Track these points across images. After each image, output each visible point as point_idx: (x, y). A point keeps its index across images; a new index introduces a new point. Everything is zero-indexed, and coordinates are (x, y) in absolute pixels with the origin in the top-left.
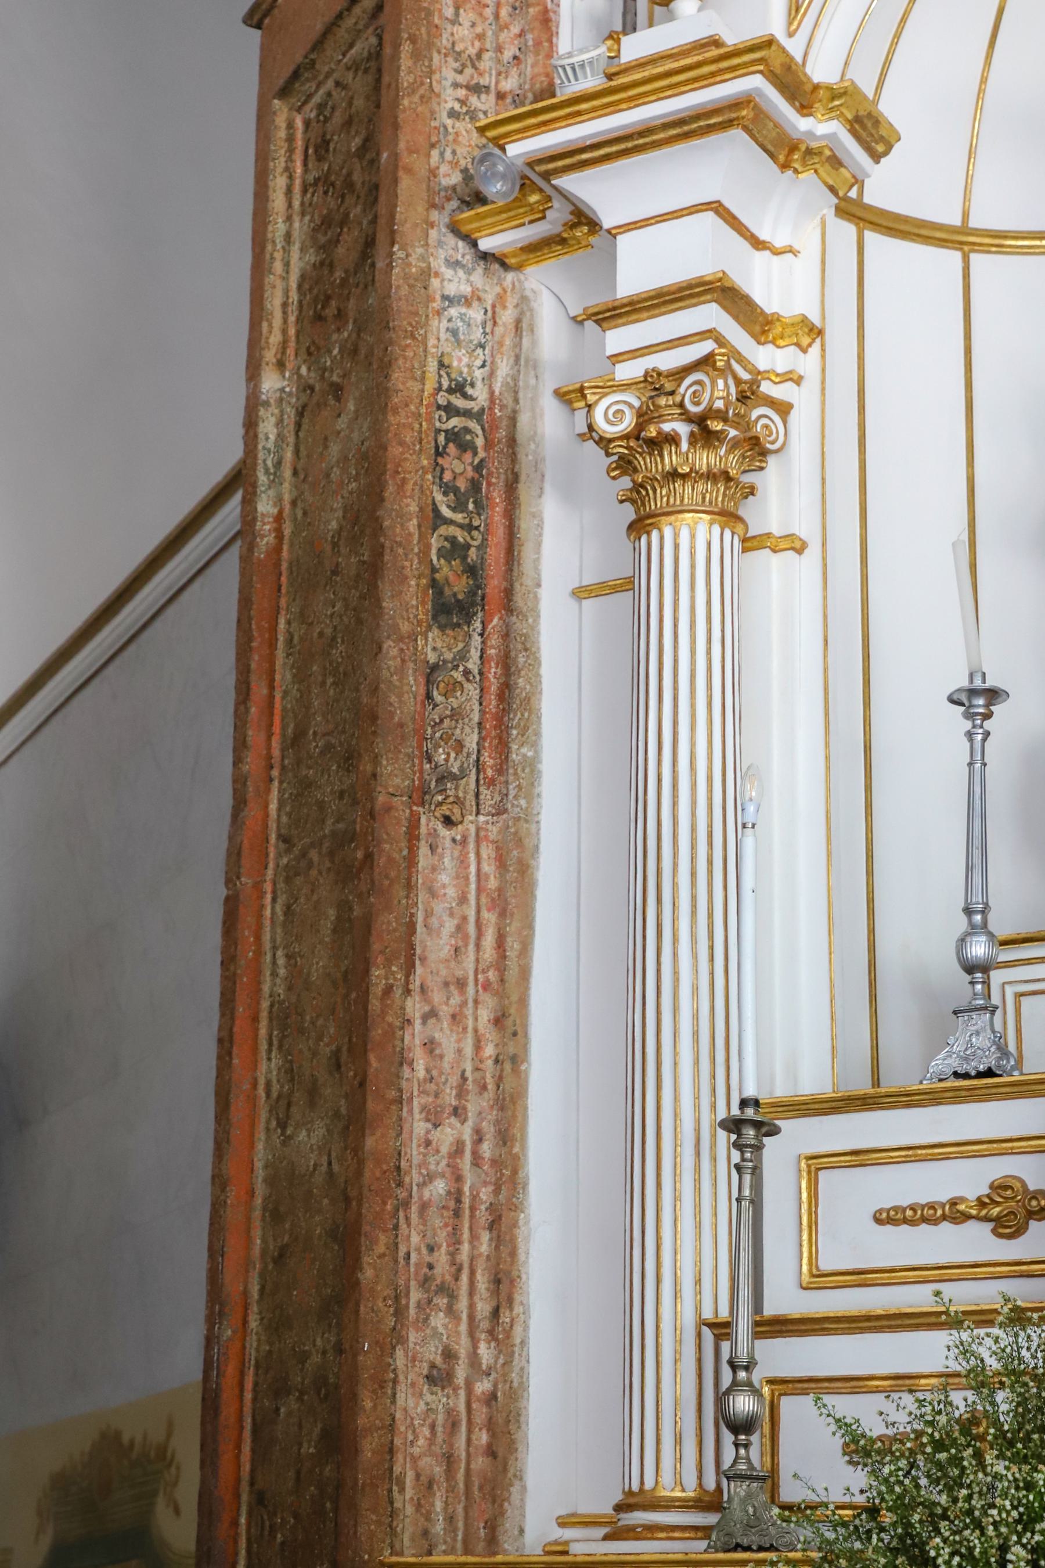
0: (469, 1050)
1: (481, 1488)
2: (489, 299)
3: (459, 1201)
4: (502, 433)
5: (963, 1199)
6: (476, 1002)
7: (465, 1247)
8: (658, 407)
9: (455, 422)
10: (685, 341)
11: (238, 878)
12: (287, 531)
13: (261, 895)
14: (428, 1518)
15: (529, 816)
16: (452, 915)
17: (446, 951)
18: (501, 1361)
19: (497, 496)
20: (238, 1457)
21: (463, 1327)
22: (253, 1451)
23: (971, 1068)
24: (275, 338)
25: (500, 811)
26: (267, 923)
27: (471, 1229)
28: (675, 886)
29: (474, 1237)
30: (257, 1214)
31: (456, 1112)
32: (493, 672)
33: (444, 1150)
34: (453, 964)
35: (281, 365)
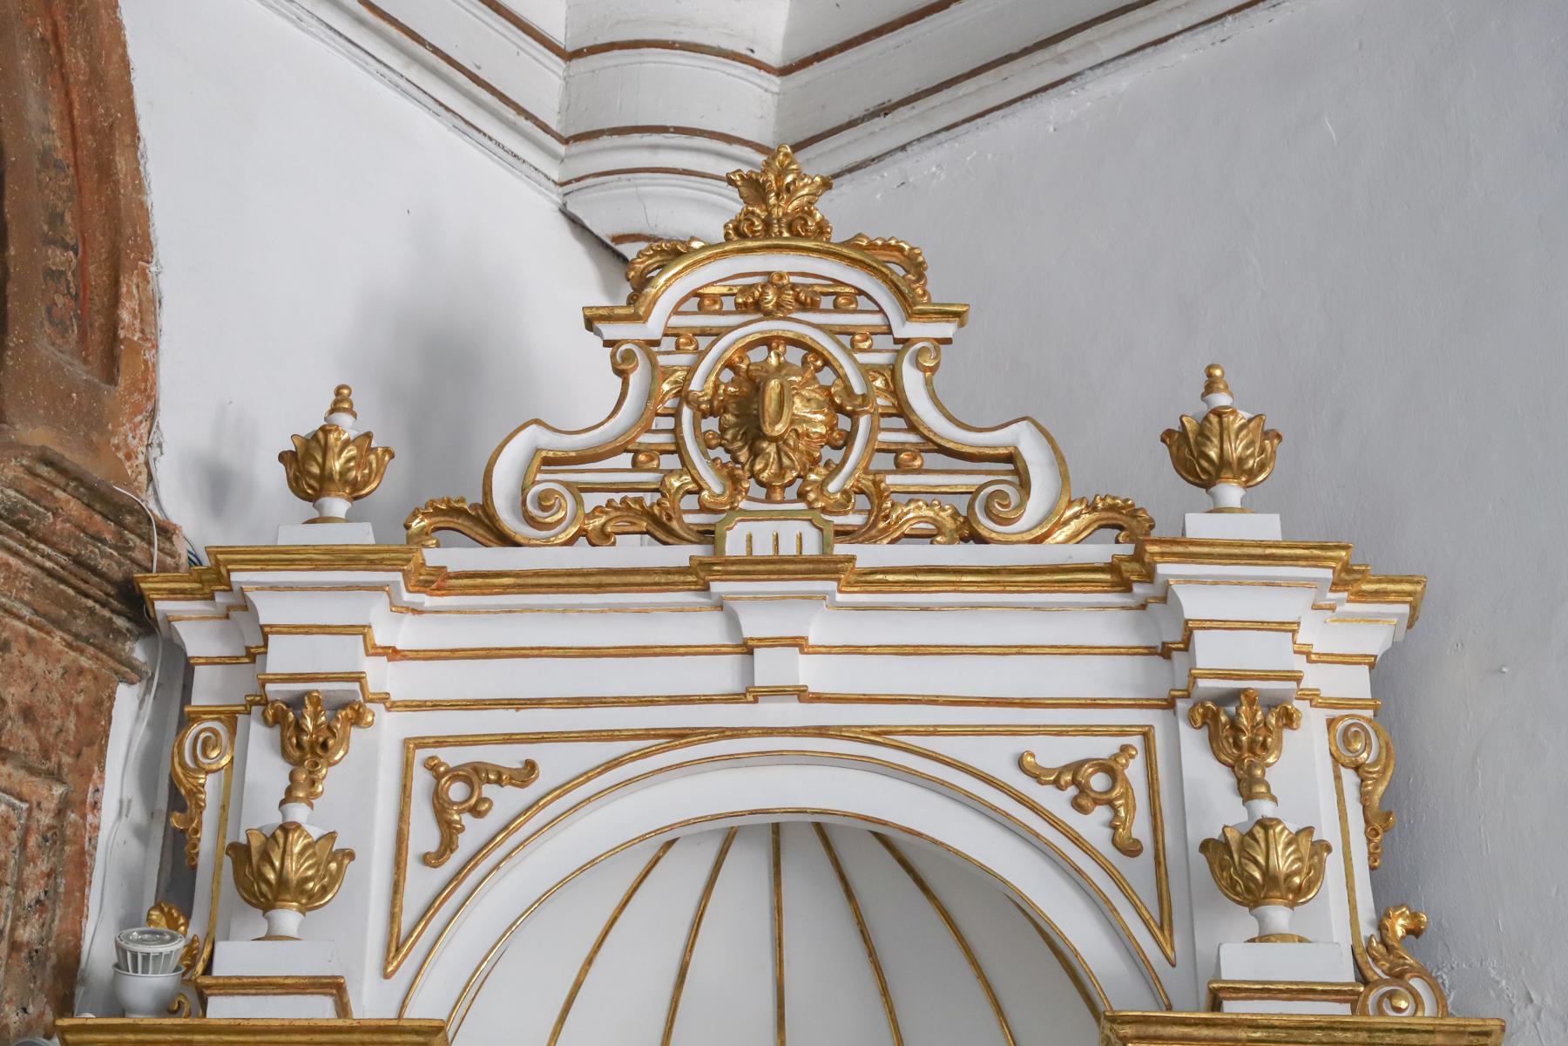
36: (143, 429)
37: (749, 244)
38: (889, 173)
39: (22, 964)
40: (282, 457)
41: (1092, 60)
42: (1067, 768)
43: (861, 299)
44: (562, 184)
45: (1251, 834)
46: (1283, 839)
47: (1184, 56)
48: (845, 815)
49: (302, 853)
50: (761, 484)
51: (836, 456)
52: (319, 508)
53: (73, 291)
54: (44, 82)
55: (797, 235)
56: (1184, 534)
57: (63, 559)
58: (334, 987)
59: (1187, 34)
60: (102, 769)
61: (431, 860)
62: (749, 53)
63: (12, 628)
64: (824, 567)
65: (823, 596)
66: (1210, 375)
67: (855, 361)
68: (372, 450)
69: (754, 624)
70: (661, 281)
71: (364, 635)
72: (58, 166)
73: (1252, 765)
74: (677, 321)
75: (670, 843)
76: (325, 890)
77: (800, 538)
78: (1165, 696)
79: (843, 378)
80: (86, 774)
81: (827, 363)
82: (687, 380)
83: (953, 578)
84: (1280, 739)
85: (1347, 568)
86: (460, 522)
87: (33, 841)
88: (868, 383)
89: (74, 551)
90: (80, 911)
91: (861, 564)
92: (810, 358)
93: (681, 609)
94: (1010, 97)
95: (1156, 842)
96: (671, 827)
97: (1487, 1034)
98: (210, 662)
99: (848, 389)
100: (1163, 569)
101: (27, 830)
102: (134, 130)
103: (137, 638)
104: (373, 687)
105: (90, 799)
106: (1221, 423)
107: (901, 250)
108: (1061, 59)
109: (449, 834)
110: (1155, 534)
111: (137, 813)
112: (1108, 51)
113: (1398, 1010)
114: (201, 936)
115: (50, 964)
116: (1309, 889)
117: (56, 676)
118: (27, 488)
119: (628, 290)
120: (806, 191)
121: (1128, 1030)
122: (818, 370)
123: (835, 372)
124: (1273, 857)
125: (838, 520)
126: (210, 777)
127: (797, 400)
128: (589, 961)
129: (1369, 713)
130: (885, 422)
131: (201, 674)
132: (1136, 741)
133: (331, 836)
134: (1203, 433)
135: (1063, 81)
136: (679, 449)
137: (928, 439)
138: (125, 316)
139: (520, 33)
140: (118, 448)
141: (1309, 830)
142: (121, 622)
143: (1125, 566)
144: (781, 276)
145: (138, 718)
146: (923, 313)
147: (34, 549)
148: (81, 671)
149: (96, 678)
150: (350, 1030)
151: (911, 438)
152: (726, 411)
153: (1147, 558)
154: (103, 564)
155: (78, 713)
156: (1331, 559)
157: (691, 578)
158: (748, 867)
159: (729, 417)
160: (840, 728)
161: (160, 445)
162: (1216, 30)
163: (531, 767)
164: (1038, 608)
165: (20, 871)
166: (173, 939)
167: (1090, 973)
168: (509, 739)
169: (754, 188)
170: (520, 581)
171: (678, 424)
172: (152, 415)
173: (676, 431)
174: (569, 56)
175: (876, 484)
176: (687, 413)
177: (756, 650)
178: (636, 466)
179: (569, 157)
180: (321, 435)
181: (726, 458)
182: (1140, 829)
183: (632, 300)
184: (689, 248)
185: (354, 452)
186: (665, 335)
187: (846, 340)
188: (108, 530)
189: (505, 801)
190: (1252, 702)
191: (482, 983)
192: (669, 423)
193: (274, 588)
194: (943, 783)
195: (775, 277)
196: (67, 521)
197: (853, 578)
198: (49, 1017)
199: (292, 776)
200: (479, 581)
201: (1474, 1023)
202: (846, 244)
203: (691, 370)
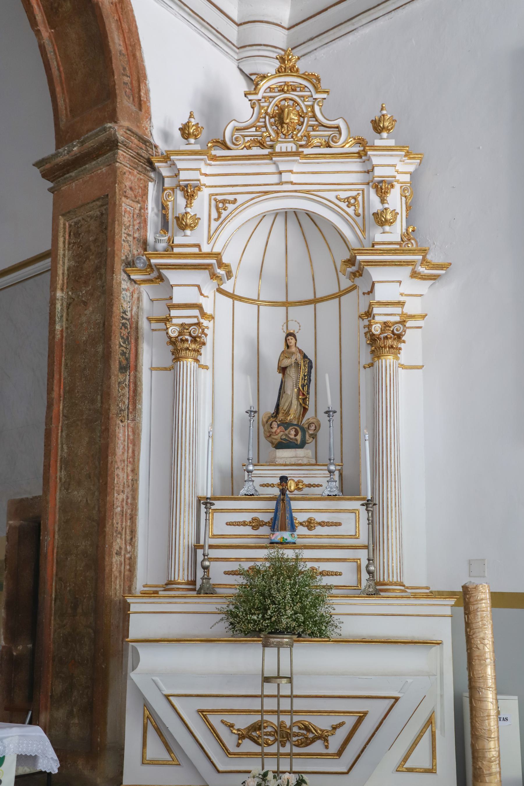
0: (125, 477)
1: (127, 579)
2: (131, 290)
3: (123, 513)
4: (134, 325)
5: (246, 522)
6: (127, 466)
7: (124, 523)
8: (184, 332)
9: (124, 321)
11: (51, 425)
12: (64, 335)
13: (58, 430)
14: (116, 585)
15: (140, 422)
16: (122, 444)
17: (121, 453)
18: (133, 550)
19: (133, 341)
20: (52, 569)
21: (124, 542)
22: (57, 568)
23: (249, 493)
24: (60, 282)
25: (134, 420)
26: (59, 437)
27: (126, 519)
28: (185, 446)
29: (126, 521)
30: (57, 510)
31: (123, 492)
32: (132, 385)
33: (120, 500)
34: (122, 456)
35: (62, 290)
36: (149, 122)
37: (281, 74)
38: (312, 56)
39: (136, 242)
40: (180, 129)
41: (360, 24)
42: (346, 198)
43: (306, 88)
44: (238, 60)
45: (383, 211)
46: (389, 212)
47: (382, 23)
48: (300, 209)
49: (190, 218)
50: (283, 134)
51: (299, 127)
52: (188, 141)
53: (130, 88)
54: (118, 32)
55: (291, 72)
56: (374, 144)
57: (135, 153)
58: (198, 246)
59: (383, 17)
60: (147, 201)
61: (216, 220)
62: (280, 24)
63: (126, 169)
64: (297, 154)
65: (296, 161)
66: (382, 106)
67: (304, 104)
68: (199, 127)
69: (282, 168)
70: (261, 84)
71: (200, 171)
72: (123, 55)
73: (384, 197)
74: (265, 94)
75: (265, 216)
76: (195, 226)
77: (292, 147)
78: (367, 182)
79: (301, 108)
80: (144, 202)
81: (298, 105)
82: (267, 109)
83: (324, 156)
84: (390, 191)
85: (408, 152)
86: (219, 145)
87: (135, 216)
88: (307, 110)
89: (137, 151)
90: (146, 231)
91: (305, 153)
92: (295, 103)
93: (266, 164)
94: (341, 35)
95: (363, 214)
96: (265, 212)
97: (426, 250)
98: (168, 177)
99: (303, 111)
100: (369, 153)
101: (134, 214)
102: (140, 45)
103: (152, 171)
104: (202, 182)
105: (146, 207)
106: (384, 118)
107: (315, 75)
108: (353, 24)
109: (219, 214)
110: (368, 145)
111: (156, 210)
112: (364, 21)
113: (408, 247)
114: (171, 236)
115: (141, 242)
116: (394, 222)
117: (136, 180)
118: (125, 136)
119: (254, 87)
120: (294, 60)
121: (356, 252)
122: (296, 106)
123: (300, 106)
124: (387, 216)
125: (300, 143)
126: (170, 202)
127: (292, 114)
128: (248, 241)
129: (409, 185)
130: (311, 119)
131: (166, 180)
132: (361, 192)
133: (196, 215)
134: (380, 121)
135: (353, 30)
136: (265, 126)
137: (320, 123)
138: (142, 94)
139: (227, 19)
140: (144, 127)
141: (395, 210)
142: (148, 168)
143: (361, 152)
144: (288, 83)
145: (154, 190)
146: (320, 92)
147: (128, 151)
148: (141, 179)
149: (144, 181)
150: (202, 254)
151: (316, 123)
152: (276, 117)
153: (366, 150)
154: (143, 155)
155: (141, 189)
156: (405, 150)
157: (269, 157)
158: (280, 221)
159: (277, 118)
160: (299, 190)
161: (153, 126)
162: (390, 15)
163: (236, 200)
164: (342, 162)
165: (133, 223)
166: (165, 236)
167: (349, 241)
168: (231, 194)
169: (282, 60)
170: (232, 158)
171: (265, 120)
172: (150, 119)
173: (265, 122)
174: (239, 25)
175: (308, 134)
176: (267, 117)
177: (282, 173)
178: (256, 131)
179: (240, 53)
180: (187, 124)
181: (276, 128)
182: (360, 211)
183: (255, 89)
184: (267, 75)
185: (195, 128)
186: (262, 98)
187: (302, 99)
188: (143, 146)
189: (230, 207)
190: (385, 183)
192: (263, 120)
193: (180, 160)
194: (321, 202)
195: (287, 83)
196: (134, 144)
197: (303, 156)
198: (142, 252)
199: (187, 202)
200: (223, 158)
201: (424, 248)
202: (302, 74)
203: (268, 107)
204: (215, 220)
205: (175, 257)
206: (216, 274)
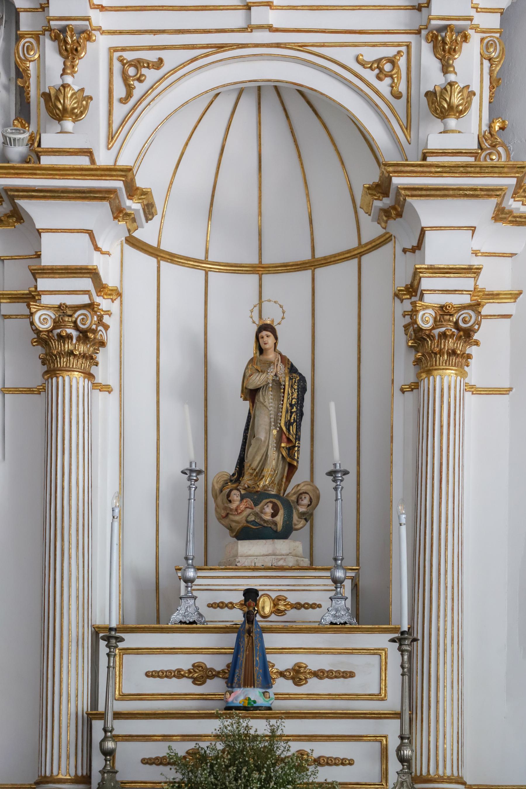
5: (183, 670)
8: (64, 321)
10: (76, 293)
28: (70, 534)
42: (375, 61)
45: (445, 89)
46: (457, 90)
48: (287, 82)
58: (88, 153)
61: (124, 101)
73: (449, 59)
75: (218, 94)
76: (82, 113)
84: (461, 47)
95: (408, 93)
98: (26, 10)
104: (94, 23)
109: (129, 89)
113: (492, 160)
114: (35, 132)
116: (465, 111)
121: (391, 169)
126: (31, 63)
128: (187, 144)
129: (498, 35)
132: (404, 49)
133: (82, 90)
141: (468, 87)
150: (96, 170)
160: (285, 44)
163: (161, 60)
166: (24, 132)
168: (151, 48)
177: (252, 8)
182: (402, 88)
190: (452, 31)
191: (146, 153)
194: (326, 68)
199: (64, 63)
204: (121, 101)
205: (43, 174)
206: (124, 209)
